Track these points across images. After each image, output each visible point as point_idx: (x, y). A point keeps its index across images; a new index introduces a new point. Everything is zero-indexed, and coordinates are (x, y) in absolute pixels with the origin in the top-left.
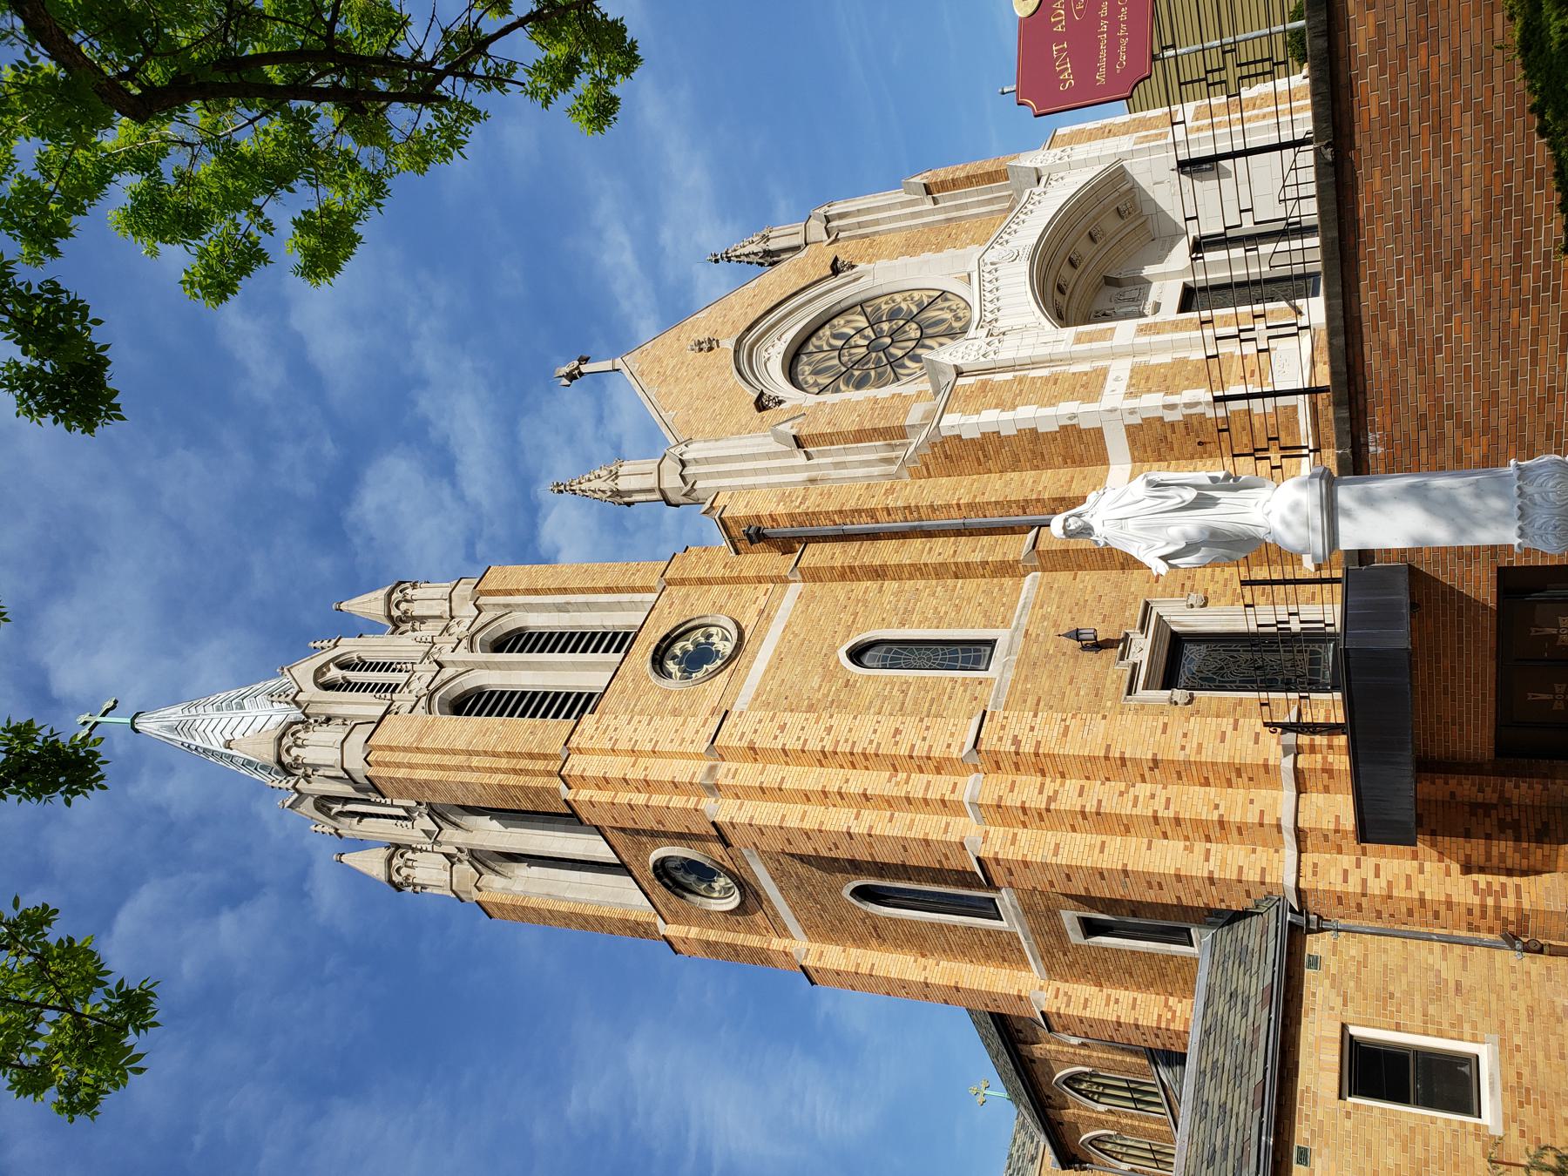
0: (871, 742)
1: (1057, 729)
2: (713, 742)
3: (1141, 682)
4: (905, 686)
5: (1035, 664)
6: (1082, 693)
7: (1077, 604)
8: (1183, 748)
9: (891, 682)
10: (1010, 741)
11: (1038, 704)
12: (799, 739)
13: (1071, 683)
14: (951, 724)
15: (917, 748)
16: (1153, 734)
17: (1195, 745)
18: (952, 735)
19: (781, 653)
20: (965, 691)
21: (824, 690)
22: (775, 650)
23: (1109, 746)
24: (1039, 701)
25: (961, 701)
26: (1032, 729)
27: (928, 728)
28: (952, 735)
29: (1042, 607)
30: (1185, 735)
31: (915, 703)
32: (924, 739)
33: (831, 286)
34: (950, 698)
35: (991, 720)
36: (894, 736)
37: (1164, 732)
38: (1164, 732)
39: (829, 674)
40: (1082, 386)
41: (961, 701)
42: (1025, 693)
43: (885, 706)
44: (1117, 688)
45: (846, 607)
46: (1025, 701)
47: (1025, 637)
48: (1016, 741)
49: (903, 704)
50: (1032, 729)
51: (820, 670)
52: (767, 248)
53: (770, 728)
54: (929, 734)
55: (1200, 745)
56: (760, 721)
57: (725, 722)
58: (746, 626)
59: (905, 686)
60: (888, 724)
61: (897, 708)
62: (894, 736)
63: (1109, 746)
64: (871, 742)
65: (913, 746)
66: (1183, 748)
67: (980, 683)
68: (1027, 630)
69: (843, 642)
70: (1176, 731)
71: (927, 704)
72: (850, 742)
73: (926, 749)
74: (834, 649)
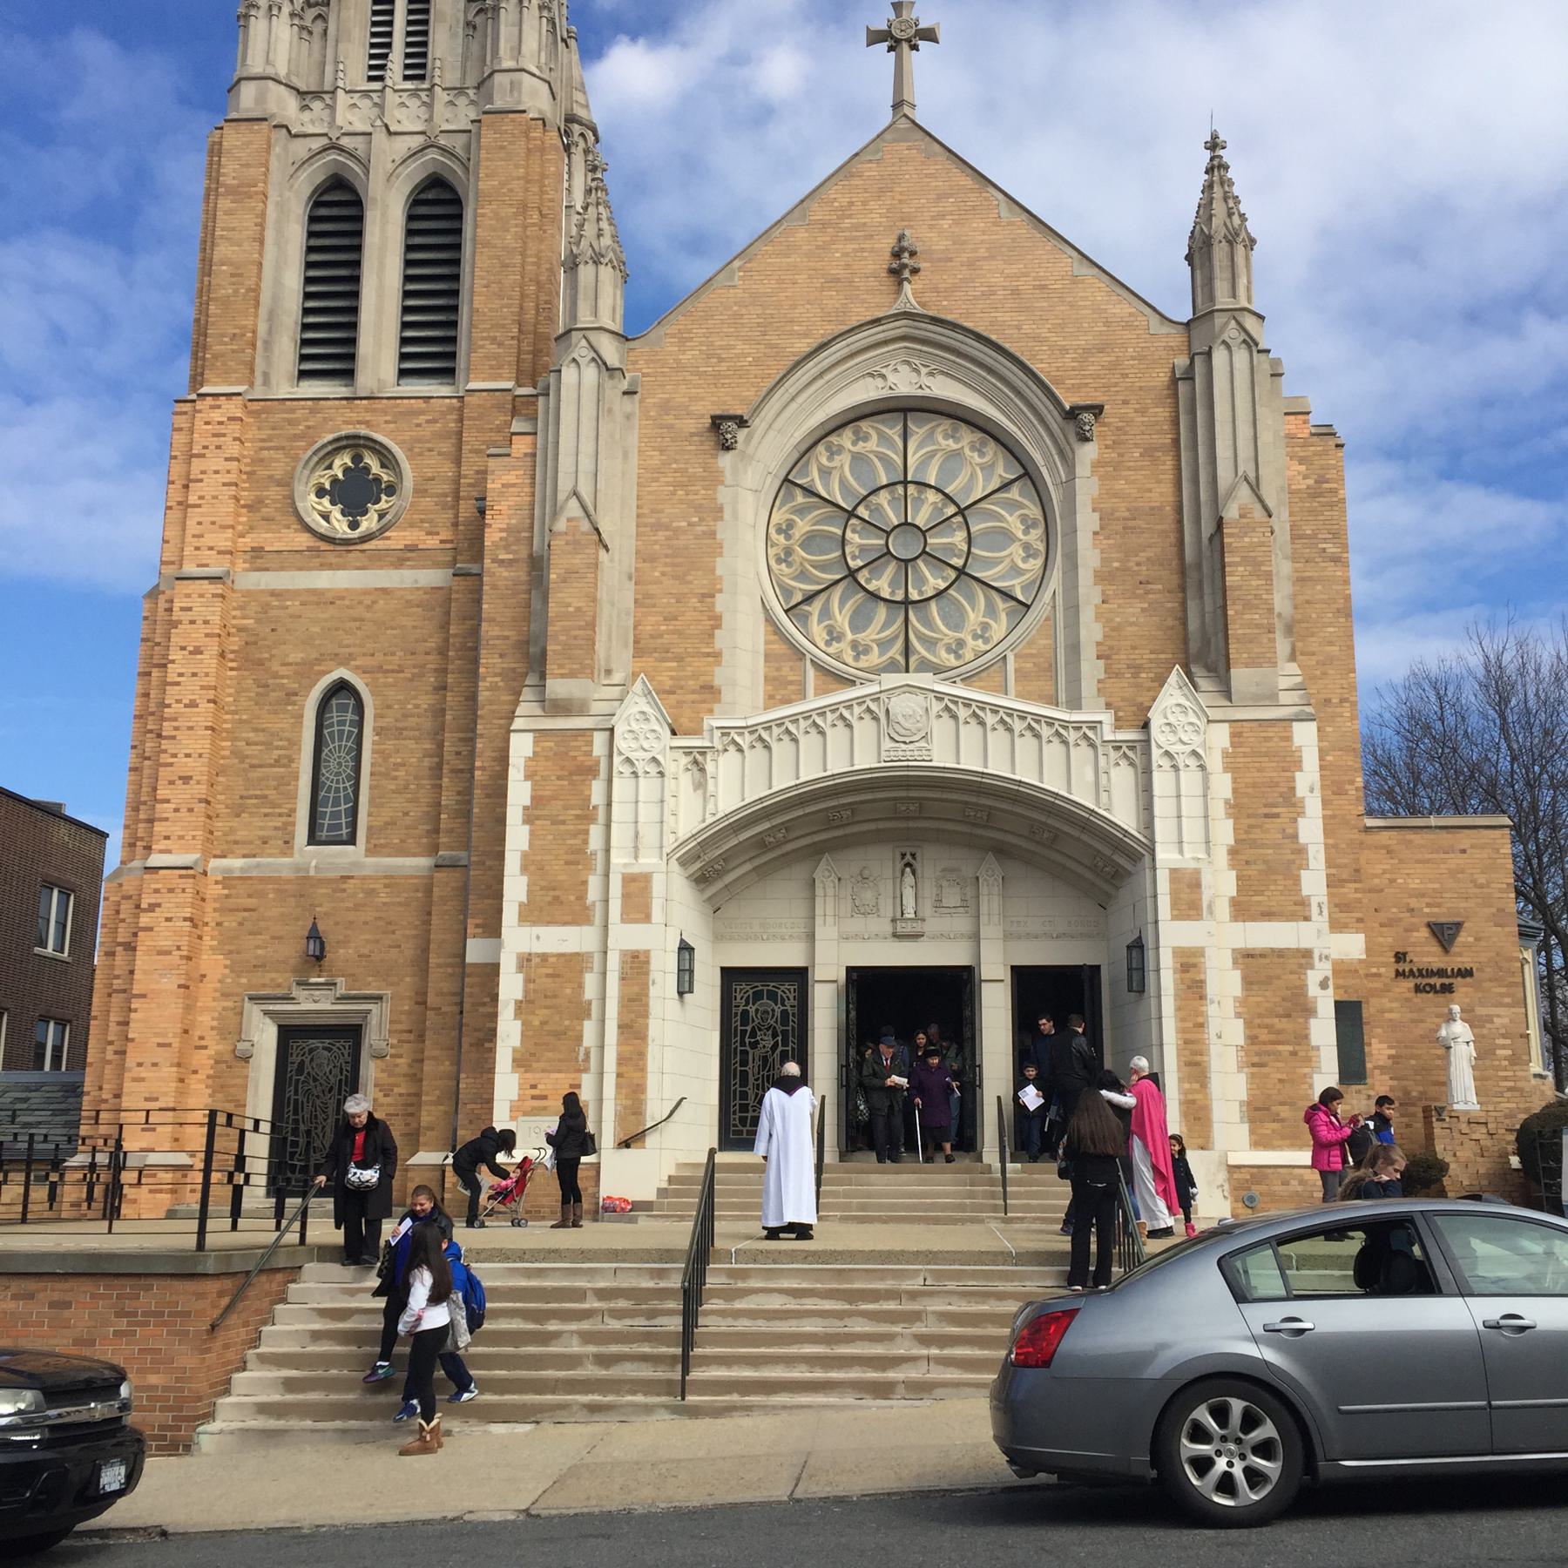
0: (174, 756)
1: (166, 944)
2: (177, 579)
3: (271, 1007)
4: (286, 761)
5: (302, 896)
6: (260, 952)
7: (390, 923)
8: (140, 1065)
9: (294, 743)
10: (153, 901)
11: (245, 910)
12: (181, 675)
13: (273, 938)
14: (194, 833)
15: (166, 805)
16: (156, 1035)
17: (143, 1075)
18: (181, 838)
19: (343, 598)
20: (276, 828)
21: (283, 671)
22: (347, 589)
23: (143, 996)
24: (253, 910)
25: (262, 828)
26: (168, 919)
27: (191, 810)
28: (181, 838)
29: (386, 886)
30: (155, 1065)
31: (260, 779)
32: (176, 810)
33: (1048, 418)
34: (266, 815)
35: (181, 877)
36: (180, 778)
37: (159, 1045)
38: (159, 1045)
39: (307, 672)
40: (556, 898)
41: (262, 828)
42: (261, 895)
43: (259, 747)
44: (264, 985)
45: (413, 654)
46: (250, 896)
47: (342, 877)
48: (152, 907)
49: (260, 766)
50: (168, 919)
51: (314, 655)
52: (1215, 242)
53: (196, 635)
54: (184, 813)
55: (142, 1080)
56: (206, 622)
57: (206, 582)
58: (388, 538)
59: (286, 761)
60: (196, 768)
61: (254, 761)
62: (180, 778)
63: (143, 996)
64: (174, 756)
65: (168, 801)
66: (140, 1065)
67: (286, 842)
68: (352, 877)
69: (357, 670)
70: (163, 1056)
71: (258, 792)
72: (174, 733)
73: (165, 815)
74: (345, 662)
